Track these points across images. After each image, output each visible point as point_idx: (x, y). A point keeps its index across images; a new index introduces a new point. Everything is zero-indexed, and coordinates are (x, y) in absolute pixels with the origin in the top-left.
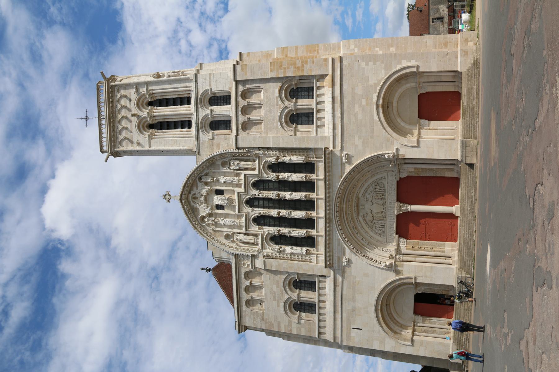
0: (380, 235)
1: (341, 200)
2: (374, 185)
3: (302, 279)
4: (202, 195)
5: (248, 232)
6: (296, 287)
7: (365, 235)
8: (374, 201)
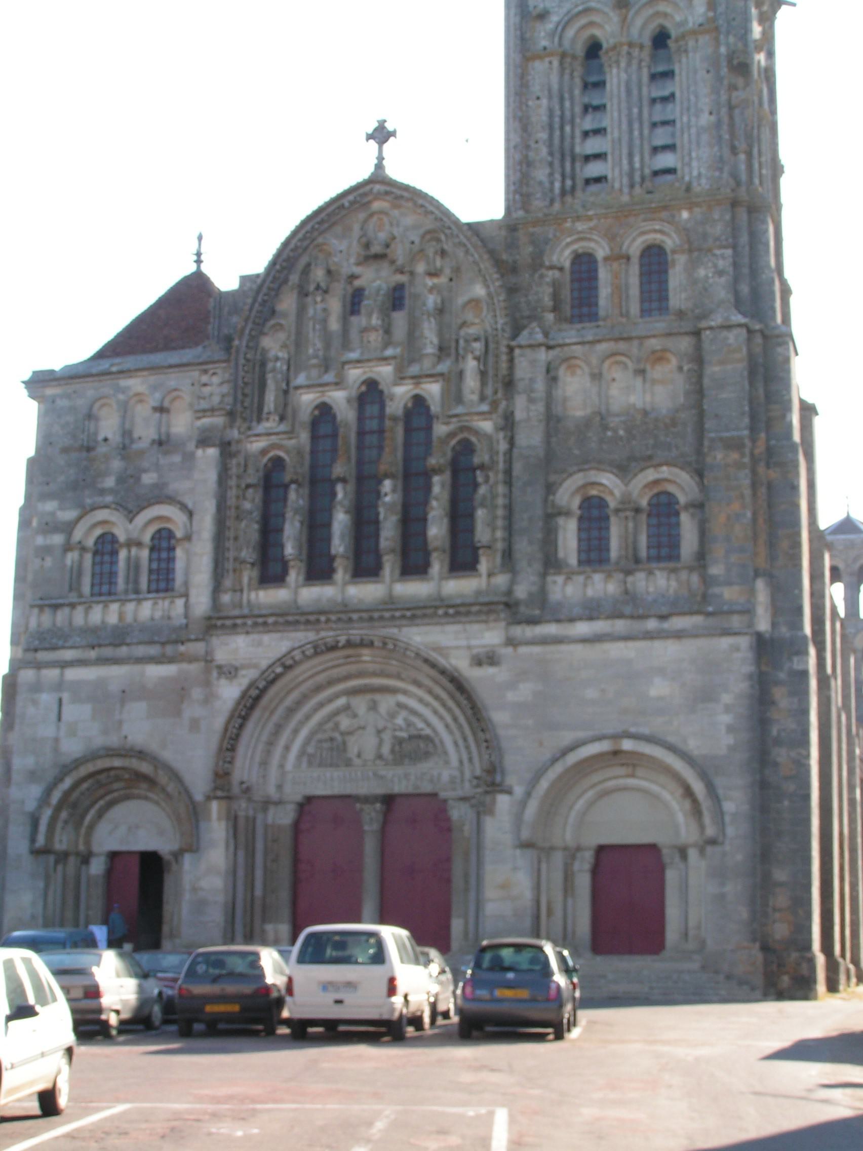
0: (302, 753)
1: (378, 648)
2: (428, 731)
3: (179, 553)
4: (387, 246)
5: (291, 390)
6: (157, 536)
7: (299, 716)
8: (387, 737)
